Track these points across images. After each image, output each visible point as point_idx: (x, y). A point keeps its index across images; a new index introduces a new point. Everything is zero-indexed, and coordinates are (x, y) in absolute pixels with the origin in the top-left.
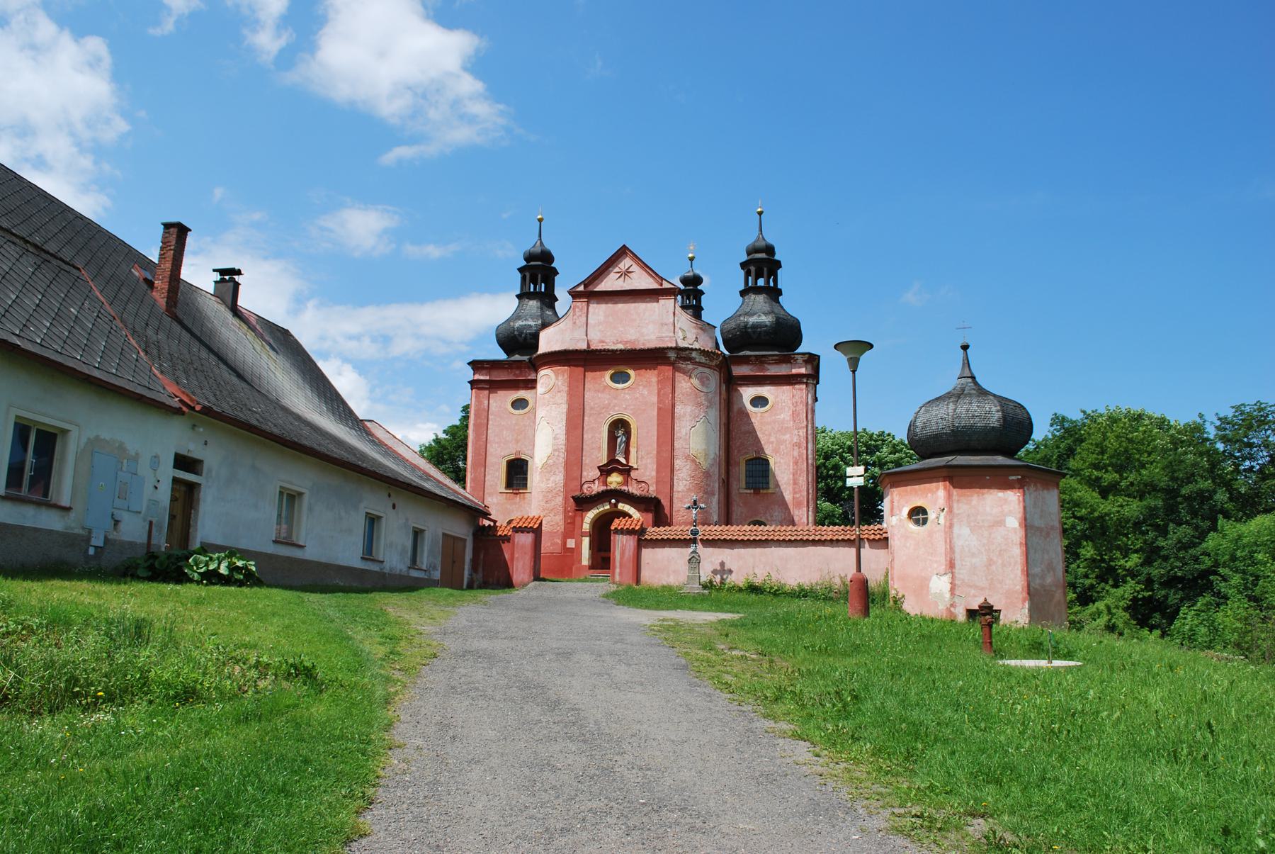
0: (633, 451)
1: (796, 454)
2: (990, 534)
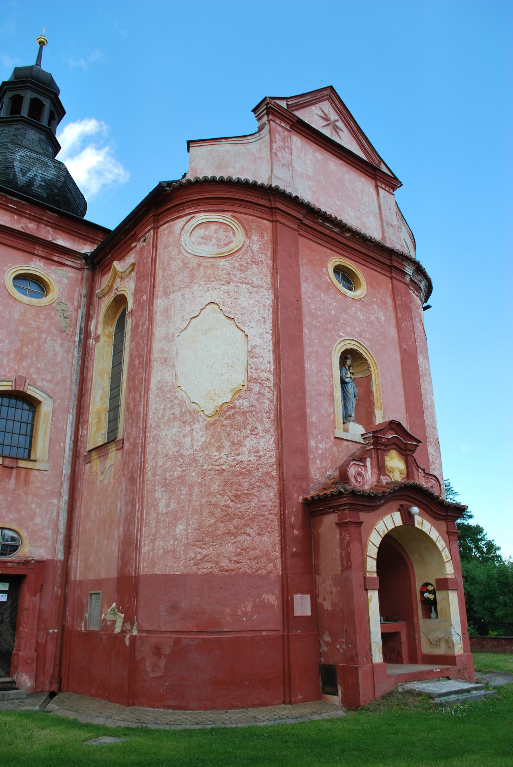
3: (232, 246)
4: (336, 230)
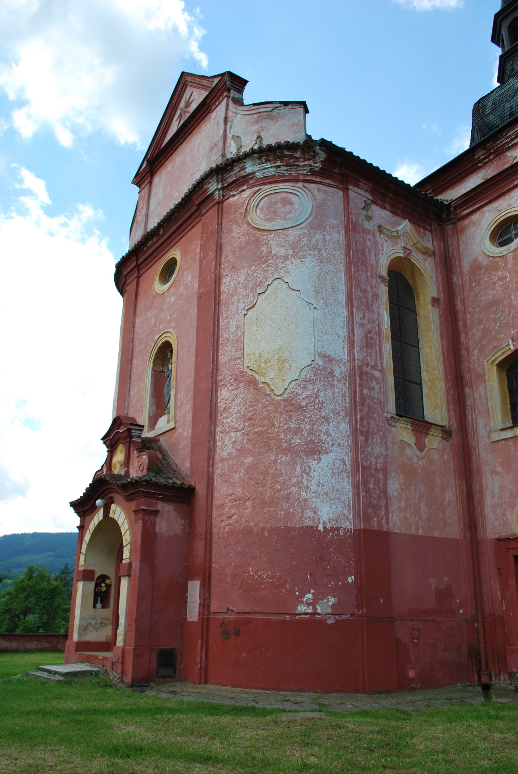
4: (155, 240)
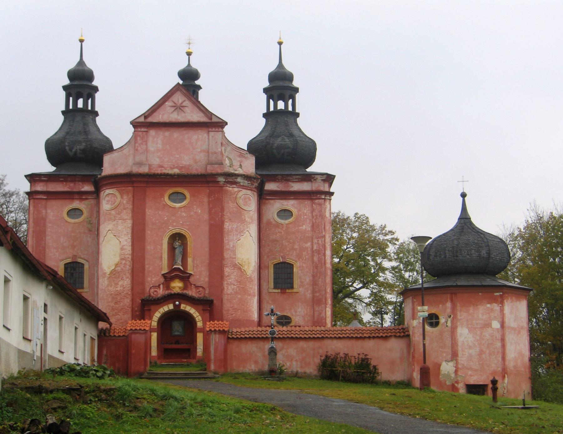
0: (190, 260)
1: (316, 259)
2: (481, 333)
3: (116, 203)
